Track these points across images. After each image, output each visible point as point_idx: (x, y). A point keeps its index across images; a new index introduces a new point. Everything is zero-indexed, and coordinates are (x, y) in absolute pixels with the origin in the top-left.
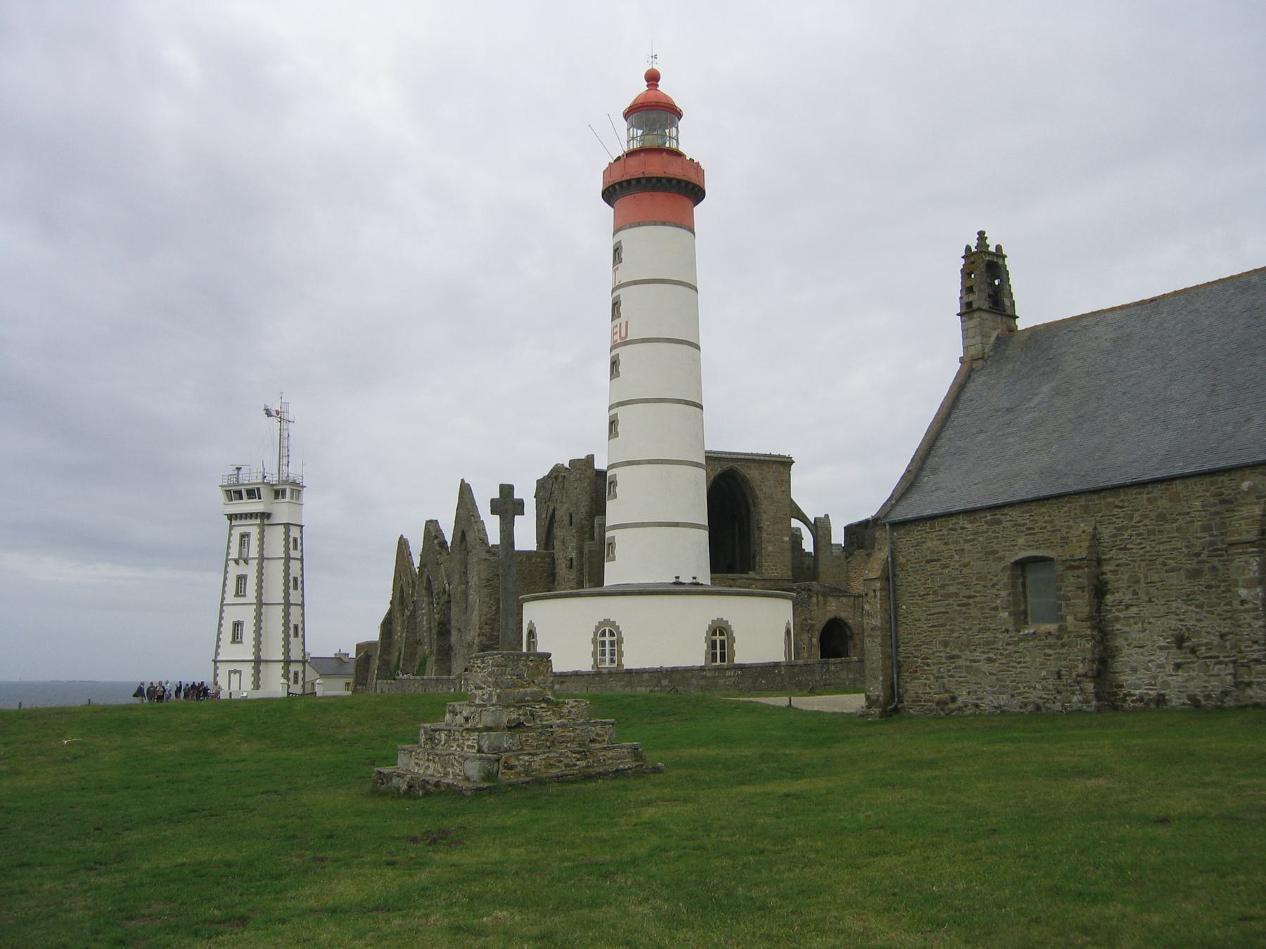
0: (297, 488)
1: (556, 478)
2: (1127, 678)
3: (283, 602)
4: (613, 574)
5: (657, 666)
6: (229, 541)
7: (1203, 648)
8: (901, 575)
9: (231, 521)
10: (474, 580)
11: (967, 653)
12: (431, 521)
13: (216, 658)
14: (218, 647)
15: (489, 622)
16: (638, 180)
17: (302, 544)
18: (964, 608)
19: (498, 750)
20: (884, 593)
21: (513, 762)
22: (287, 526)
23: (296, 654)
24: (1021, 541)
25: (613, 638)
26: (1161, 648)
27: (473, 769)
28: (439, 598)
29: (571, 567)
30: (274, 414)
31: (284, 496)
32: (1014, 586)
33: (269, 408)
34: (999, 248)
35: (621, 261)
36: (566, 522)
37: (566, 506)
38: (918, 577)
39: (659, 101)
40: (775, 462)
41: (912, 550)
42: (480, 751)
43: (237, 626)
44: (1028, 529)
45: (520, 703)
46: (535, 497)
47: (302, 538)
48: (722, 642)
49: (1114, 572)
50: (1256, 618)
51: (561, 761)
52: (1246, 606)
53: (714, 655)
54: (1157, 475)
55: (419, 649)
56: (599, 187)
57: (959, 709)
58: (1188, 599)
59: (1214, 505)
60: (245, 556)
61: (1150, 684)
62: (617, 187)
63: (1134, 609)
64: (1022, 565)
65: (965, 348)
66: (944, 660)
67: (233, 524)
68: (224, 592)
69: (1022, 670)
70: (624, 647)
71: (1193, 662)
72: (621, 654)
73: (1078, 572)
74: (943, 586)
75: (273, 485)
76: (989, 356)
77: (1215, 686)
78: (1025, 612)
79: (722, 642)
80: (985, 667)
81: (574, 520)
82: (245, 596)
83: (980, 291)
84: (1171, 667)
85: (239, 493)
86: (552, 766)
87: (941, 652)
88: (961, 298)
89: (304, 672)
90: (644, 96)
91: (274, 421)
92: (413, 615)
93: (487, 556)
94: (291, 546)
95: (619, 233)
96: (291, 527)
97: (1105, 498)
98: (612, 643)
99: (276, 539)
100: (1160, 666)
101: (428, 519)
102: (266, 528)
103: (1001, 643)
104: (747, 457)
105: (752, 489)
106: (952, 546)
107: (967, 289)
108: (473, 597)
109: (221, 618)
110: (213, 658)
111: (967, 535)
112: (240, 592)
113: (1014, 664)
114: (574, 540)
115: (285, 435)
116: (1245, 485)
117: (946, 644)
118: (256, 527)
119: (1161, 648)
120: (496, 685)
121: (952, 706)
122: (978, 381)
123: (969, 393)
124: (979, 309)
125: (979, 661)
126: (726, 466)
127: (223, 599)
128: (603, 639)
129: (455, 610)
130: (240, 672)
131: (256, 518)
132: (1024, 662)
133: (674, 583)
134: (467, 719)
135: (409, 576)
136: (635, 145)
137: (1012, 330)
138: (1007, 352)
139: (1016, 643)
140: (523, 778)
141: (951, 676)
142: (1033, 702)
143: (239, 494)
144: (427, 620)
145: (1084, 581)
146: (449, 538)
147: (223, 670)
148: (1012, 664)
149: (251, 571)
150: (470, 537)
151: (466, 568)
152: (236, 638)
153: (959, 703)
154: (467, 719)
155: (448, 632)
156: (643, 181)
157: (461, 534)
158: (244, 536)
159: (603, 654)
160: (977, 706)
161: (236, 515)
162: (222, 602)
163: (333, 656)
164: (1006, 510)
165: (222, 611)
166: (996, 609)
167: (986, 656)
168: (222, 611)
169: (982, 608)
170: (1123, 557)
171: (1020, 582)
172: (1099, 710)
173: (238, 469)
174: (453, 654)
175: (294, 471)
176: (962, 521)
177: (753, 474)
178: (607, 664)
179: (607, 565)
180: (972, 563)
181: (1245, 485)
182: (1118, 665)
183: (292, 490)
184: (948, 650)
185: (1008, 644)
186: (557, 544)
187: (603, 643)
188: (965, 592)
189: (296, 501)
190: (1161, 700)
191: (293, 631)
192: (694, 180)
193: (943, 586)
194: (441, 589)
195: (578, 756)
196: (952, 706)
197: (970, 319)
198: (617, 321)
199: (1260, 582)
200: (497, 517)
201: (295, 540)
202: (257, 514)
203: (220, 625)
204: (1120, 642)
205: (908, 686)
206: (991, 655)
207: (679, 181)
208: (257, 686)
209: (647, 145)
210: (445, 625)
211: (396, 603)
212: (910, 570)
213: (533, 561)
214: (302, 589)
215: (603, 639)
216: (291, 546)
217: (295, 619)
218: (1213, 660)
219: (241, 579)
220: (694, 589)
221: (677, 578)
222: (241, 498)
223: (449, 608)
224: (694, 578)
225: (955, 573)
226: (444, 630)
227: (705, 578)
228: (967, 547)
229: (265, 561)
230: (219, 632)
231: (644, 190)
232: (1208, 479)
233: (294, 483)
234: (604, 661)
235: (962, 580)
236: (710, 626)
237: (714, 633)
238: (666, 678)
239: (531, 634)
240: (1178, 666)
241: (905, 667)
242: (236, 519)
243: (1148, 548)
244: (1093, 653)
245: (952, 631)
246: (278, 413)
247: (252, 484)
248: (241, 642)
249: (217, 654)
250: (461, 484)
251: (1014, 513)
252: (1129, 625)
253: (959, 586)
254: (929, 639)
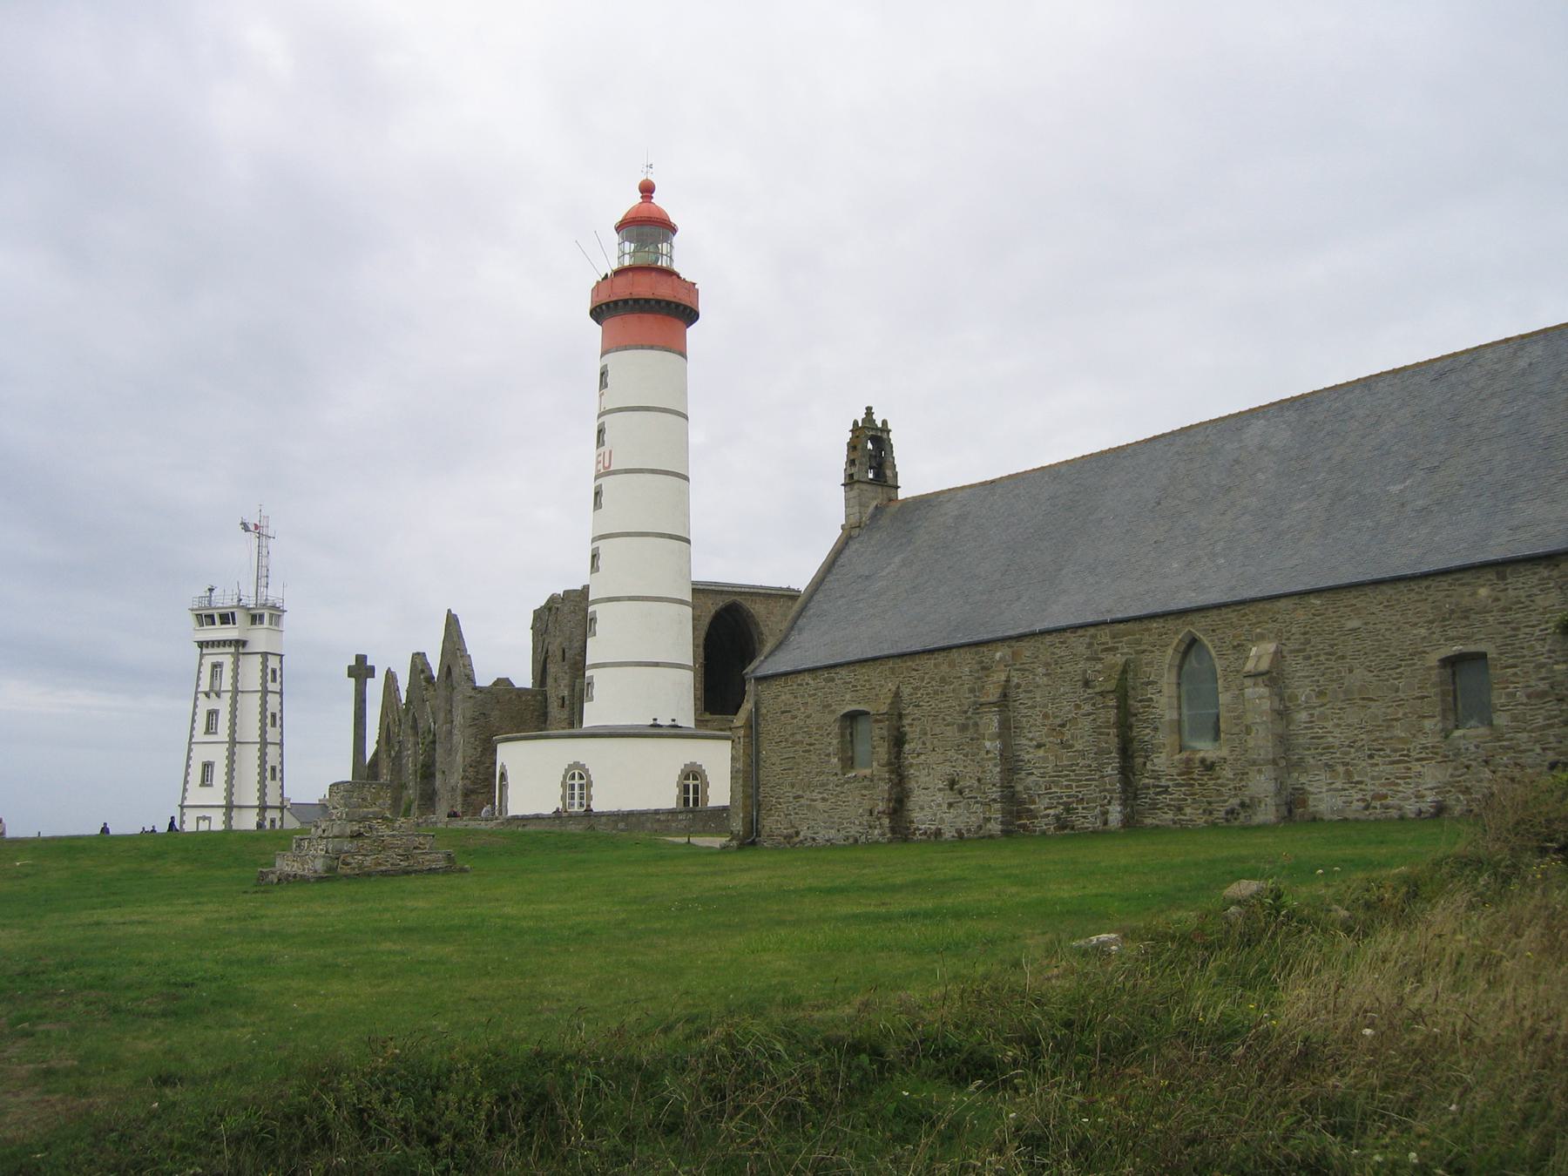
0: (277, 613)
1: (550, 609)
2: (917, 815)
3: (259, 740)
4: (593, 715)
5: (615, 809)
6: (199, 672)
7: (967, 790)
8: (763, 723)
9: (202, 649)
10: (458, 720)
11: (808, 793)
12: (418, 654)
13: (183, 802)
14: (185, 790)
15: (474, 764)
16: (626, 301)
17: (281, 676)
18: (806, 754)
19: (340, 851)
20: (747, 740)
21: (349, 860)
22: (265, 655)
23: (272, 799)
24: (848, 697)
25: (582, 782)
26: (940, 790)
27: (319, 865)
28: (424, 738)
29: (563, 706)
30: (252, 528)
31: (262, 622)
32: (843, 735)
33: (246, 521)
34: (885, 422)
35: (606, 386)
36: (559, 658)
37: (559, 640)
38: (775, 726)
39: (651, 216)
40: (783, 596)
41: (771, 702)
42: (327, 852)
43: (207, 767)
44: (853, 686)
45: (364, 819)
46: (532, 628)
47: (281, 669)
48: (696, 788)
49: (911, 725)
50: (995, 766)
51: (388, 861)
52: (990, 755)
53: (686, 801)
54: (941, 644)
55: (405, 793)
56: (588, 306)
57: (801, 842)
58: (959, 748)
59: (978, 672)
60: (217, 688)
61: (932, 820)
62: (604, 307)
63: (923, 757)
64: (852, 717)
65: (847, 516)
66: (791, 800)
67: (204, 652)
68: (192, 728)
69: (847, 808)
70: (593, 791)
71: (960, 802)
72: (590, 798)
73: (881, 725)
74: (793, 734)
75: (249, 609)
76: (866, 525)
77: (974, 821)
78: (852, 759)
79: (696, 788)
80: (820, 805)
81: (567, 655)
82: (216, 733)
83: (860, 464)
84: (946, 805)
85: (212, 617)
86: (380, 864)
87: (789, 792)
88: (845, 470)
89: (282, 819)
90: (636, 209)
91: (253, 536)
92: (399, 755)
93: (473, 693)
94: (269, 677)
95: (607, 356)
96: (269, 656)
97: (906, 662)
98: (581, 787)
99: (252, 671)
100: (939, 805)
101: (415, 652)
102: (241, 657)
103: (832, 785)
104: (752, 590)
105: (757, 624)
106: (799, 700)
107: (851, 462)
108: (458, 737)
109: (189, 758)
110: (180, 803)
111: (810, 690)
112: (210, 728)
113: (841, 803)
114: (567, 677)
115: (264, 552)
116: (998, 655)
117: (793, 786)
118: (230, 656)
119: (940, 790)
120: (346, 805)
121: (796, 840)
122: (854, 546)
123: (842, 560)
124: (858, 481)
125: (815, 801)
126: (728, 600)
127: (192, 736)
128: (573, 782)
129: (439, 751)
130: (209, 819)
131: (230, 646)
132: (848, 801)
133: (652, 726)
134: (324, 831)
135: (395, 713)
136: (627, 262)
137: (892, 499)
138: (880, 522)
139: (842, 785)
140: (357, 871)
141: (797, 814)
142: (853, 836)
144: (412, 760)
145: (885, 733)
146: (436, 673)
148: (839, 803)
149: (223, 705)
150: (456, 672)
151: (451, 705)
152: (206, 781)
153: (801, 837)
154: (324, 831)
155: (433, 775)
156: (631, 303)
157: (447, 670)
158: (216, 666)
159: (573, 798)
160: (814, 839)
161: (207, 642)
162: (190, 739)
163: (318, 802)
164: (838, 670)
165: (190, 750)
166: (828, 755)
167: (821, 796)
168: (190, 750)
169: (820, 754)
170: (917, 713)
171: (848, 732)
172: (890, 841)
173: (211, 590)
174: (437, 799)
175: (273, 594)
176: (808, 678)
177: (758, 609)
178: (576, 808)
179: (586, 705)
180: (813, 715)
181: (998, 655)
182: (910, 805)
183: (271, 616)
184: (794, 790)
185: (837, 786)
186: (550, 681)
187: (572, 787)
188: (807, 740)
189: (276, 628)
190: (938, 833)
191: (270, 772)
192: (686, 301)
193: (793, 734)
194: (426, 728)
195: (402, 858)
196: (796, 840)
197: (851, 490)
198: (602, 449)
199: (1000, 736)
200: (353, 680)
201: (274, 671)
202: (231, 641)
203: (188, 766)
204: (913, 784)
205: (765, 822)
206: (825, 795)
207: (668, 303)
209: (639, 263)
210: (429, 767)
211: (383, 743)
212: (769, 720)
213: (524, 699)
214: (281, 726)
215: (573, 782)
216: (269, 677)
217: (272, 759)
218: (973, 800)
219: (212, 714)
220: (674, 732)
221: (655, 720)
222: (214, 624)
223: (435, 749)
224: (674, 720)
225: (801, 723)
226: (427, 773)
227: (687, 720)
228: (810, 700)
229: (239, 694)
230: (187, 774)
231: (632, 311)
232: (974, 650)
233: (274, 607)
234: (573, 805)
235: (806, 730)
236: (682, 770)
237: (687, 778)
238: (622, 821)
239: (503, 776)
240: (950, 805)
241: (762, 807)
242: (207, 647)
243: (933, 706)
244: (890, 794)
245: (798, 774)
246: (256, 527)
247: (226, 608)
248: (211, 785)
249: (184, 798)
250: (448, 615)
251: (843, 672)
252: (919, 771)
253: (804, 735)
254: (781, 781)
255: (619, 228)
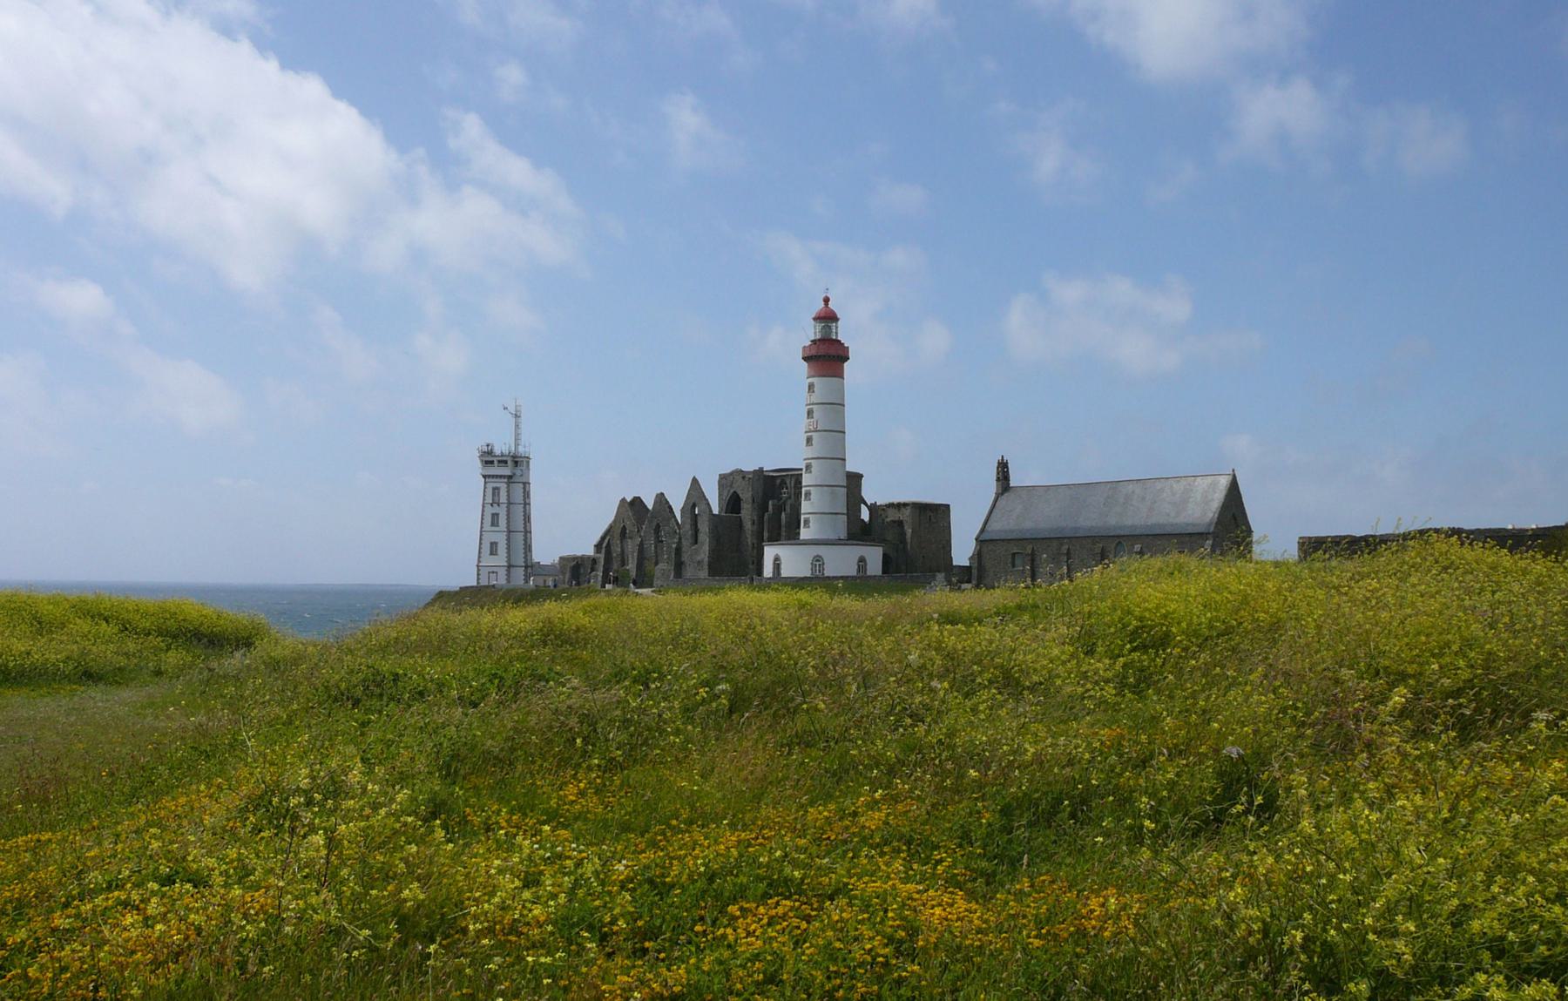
4: (804, 534)
22: (524, 484)
64: (1014, 554)
85: (492, 462)
143: (492, 462)
147: (484, 572)
168: (481, 535)
175: (521, 449)
191: (528, 548)
208: (508, 580)
219: (495, 516)
255: (815, 319)
